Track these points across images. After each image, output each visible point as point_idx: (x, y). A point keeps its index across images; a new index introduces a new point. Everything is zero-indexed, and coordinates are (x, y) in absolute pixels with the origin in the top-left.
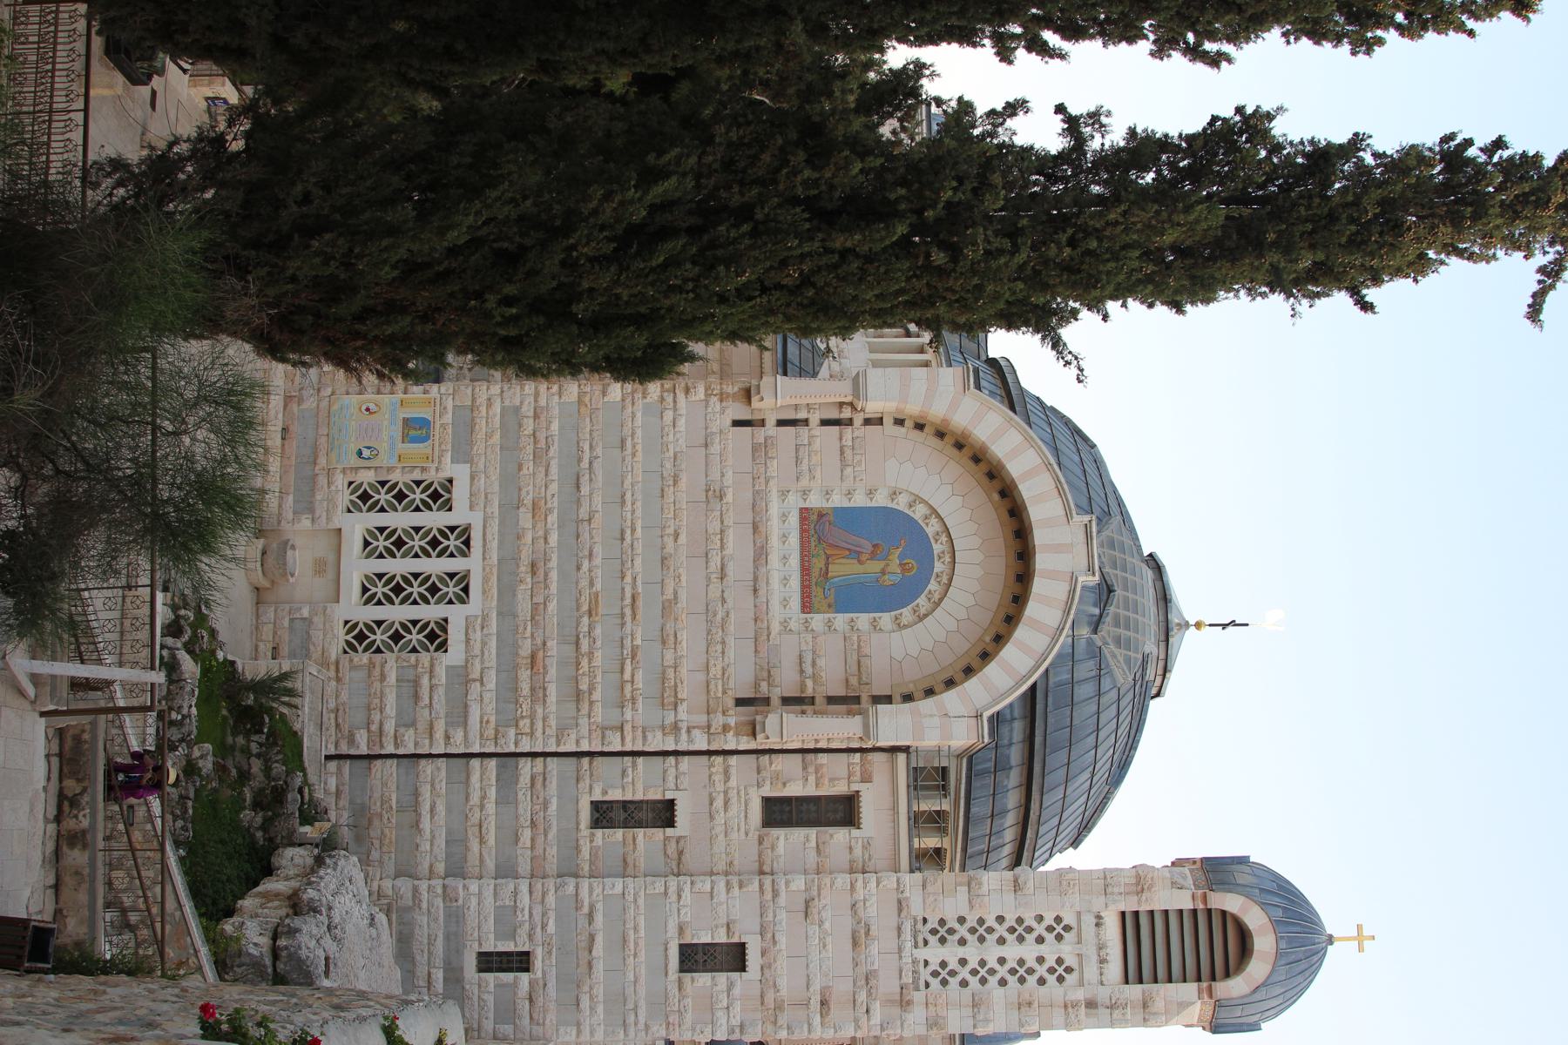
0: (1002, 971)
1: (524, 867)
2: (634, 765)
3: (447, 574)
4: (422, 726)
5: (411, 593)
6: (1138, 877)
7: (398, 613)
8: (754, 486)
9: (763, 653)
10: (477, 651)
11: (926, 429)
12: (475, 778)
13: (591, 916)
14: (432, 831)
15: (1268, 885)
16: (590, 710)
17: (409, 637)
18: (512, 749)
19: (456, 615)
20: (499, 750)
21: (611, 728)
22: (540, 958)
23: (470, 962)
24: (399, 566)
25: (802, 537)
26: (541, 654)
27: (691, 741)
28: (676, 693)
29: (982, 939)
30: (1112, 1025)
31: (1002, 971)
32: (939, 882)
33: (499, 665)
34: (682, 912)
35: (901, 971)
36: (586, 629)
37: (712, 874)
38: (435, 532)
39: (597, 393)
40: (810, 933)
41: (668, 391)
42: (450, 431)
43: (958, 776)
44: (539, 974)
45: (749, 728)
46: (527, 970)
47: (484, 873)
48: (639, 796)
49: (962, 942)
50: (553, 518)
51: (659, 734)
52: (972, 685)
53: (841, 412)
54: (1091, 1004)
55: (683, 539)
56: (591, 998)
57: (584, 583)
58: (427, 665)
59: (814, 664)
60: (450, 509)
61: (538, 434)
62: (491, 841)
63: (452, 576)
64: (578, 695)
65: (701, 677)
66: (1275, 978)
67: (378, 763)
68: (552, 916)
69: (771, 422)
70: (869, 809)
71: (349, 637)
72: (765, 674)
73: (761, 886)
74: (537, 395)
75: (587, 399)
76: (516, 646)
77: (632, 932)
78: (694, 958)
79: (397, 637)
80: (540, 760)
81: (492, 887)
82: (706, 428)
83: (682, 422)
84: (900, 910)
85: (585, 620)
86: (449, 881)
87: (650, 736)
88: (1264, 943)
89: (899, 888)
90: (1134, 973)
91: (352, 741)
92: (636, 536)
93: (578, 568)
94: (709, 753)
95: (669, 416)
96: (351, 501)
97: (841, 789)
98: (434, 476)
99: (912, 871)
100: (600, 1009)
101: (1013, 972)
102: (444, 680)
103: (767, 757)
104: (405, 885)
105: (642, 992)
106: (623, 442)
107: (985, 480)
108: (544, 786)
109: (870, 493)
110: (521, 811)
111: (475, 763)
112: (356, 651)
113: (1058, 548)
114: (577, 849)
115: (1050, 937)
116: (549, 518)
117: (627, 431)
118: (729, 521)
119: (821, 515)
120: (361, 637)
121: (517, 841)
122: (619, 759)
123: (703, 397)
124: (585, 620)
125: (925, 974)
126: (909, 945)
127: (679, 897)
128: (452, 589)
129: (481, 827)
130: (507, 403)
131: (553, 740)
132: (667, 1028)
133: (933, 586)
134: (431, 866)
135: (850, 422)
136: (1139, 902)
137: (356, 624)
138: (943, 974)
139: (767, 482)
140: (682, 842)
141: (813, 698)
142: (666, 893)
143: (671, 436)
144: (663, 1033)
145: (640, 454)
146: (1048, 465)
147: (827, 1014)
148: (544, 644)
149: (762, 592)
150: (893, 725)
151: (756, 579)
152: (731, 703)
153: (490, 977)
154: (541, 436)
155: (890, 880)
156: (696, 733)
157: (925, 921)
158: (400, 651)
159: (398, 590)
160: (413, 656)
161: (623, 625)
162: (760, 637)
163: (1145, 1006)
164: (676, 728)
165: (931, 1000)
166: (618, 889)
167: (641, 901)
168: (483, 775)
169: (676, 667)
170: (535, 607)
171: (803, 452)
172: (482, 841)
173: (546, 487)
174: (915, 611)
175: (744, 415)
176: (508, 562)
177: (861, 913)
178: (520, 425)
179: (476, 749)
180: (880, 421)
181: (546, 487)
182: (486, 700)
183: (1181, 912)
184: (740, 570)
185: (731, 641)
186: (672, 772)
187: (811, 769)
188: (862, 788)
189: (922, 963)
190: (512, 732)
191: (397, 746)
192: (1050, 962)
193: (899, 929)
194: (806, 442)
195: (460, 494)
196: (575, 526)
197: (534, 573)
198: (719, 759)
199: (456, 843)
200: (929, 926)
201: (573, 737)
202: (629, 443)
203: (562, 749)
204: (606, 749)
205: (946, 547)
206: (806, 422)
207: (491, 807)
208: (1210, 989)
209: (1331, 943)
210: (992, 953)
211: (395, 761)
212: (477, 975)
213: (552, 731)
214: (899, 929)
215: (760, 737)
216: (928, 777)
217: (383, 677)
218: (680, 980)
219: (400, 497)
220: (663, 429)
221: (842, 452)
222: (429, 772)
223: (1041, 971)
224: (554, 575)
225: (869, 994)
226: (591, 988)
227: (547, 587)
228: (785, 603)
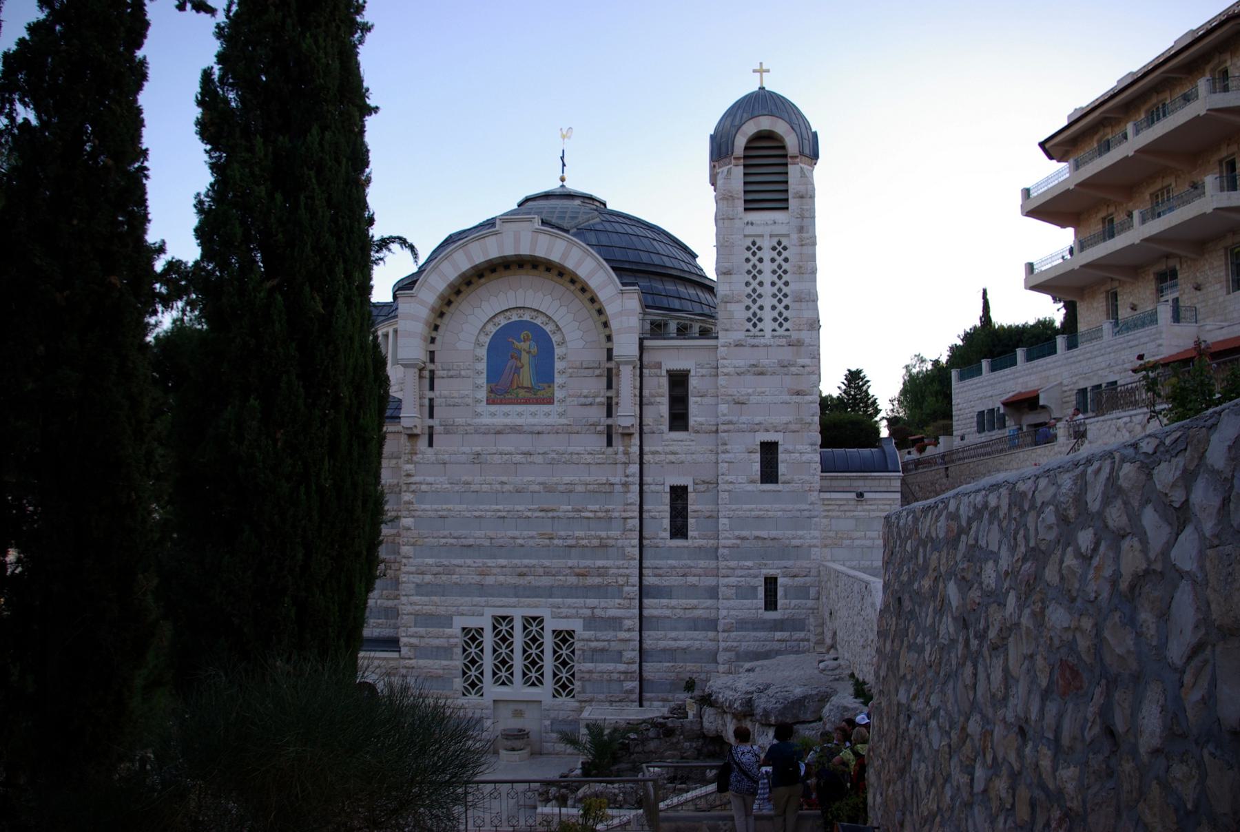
0: (780, 284)
1: (711, 581)
2: (649, 511)
3: (524, 631)
4: (619, 646)
5: (536, 654)
6: (722, 199)
7: (548, 663)
8: (471, 434)
9: (579, 428)
10: (574, 611)
11: (438, 323)
12: (655, 612)
13: (743, 538)
14: (688, 640)
15: (729, 119)
16: (613, 539)
17: (564, 656)
18: (637, 588)
19: (550, 625)
20: (638, 597)
21: (625, 524)
22: (768, 571)
23: (771, 615)
24: (518, 662)
25: (505, 404)
26: (577, 570)
27: (633, 475)
28: (602, 484)
29: (760, 296)
30: (813, 218)
31: (780, 284)
32: (725, 321)
33: (583, 597)
34: (741, 481)
35: (779, 346)
36: (561, 541)
37: (717, 463)
38: (496, 639)
39: (408, 534)
40: (755, 401)
41: (408, 488)
42: (430, 629)
43: (657, 315)
44: (779, 571)
45: (626, 438)
46: (776, 579)
47: (715, 606)
48: (668, 508)
49: (761, 308)
50: (490, 562)
51: (629, 495)
52: (602, 296)
53: (425, 378)
54: (801, 229)
55: (504, 479)
56: (794, 538)
57: (531, 542)
58: (582, 643)
59: (585, 397)
60: (482, 629)
61: (434, 572)
62: (695, 602)
63: (525, 628)
64: (603, 546)
65: (593, 468)
66: (787, 119)
67: (645, 674)
68: (741, 563)
69: (430, 422)
70: (678, 364)
71: (564, 694)
72: (592, 427)
73: (725, 431)
74: (408, 573)
75: (412, 540)
76: (571, 587)
77: (753, 513)
78: (769, 473)
79: (564, 664)
80: (645, 571)
81: (725, 601)
82: (433, 463)
83: (430, 479)
84: (742, 345)
85: (556, 542)
86: (720, 628)
87: (630, 501)
88: (765, 123)
89: (728, 345)
90: (781, 204)
91: (631, 691)
92: (502, 509)
93: (522, 546)
94: (641, 464)
95: (424, 487)
96: (476, 694)
97: (665, 382)
98: (459, 640)
99: (717, 338)
100: (800, 533)
101: (780, 277)
102: (592, 632)
103: (644, 428)
104: (721, 657)
105: (790, 507)
106: (441, 517)
107: (472, 287)
108: (661, 568)
109: (478, 359)
110: (676, 583)
111: (645, 613)
112: (573, 690)
113: (517, 240)
114: (700, 548)
115: (759, 254)
116: (489, 565)
117: (432, 514)
118: (493, 450)
119: (491, 391)
120: (564, 687)
121: (695, 586)
122: (645, 522)
123: (413, 466)
124: (556, 542)
125: (781, 331)
126: (763, 341)
127: (731, 483)
128: (534, 628)
129: (686, 609)
130: (413, 592)
131: (632, 562)
132: (813, 491)
133: (538, 322)
134: (710, 640)
135: (432, 372)
136: (739, 199)
137: (556, 690)
138: (780, 320)
139: (469, 425)
140: (697, 481)
141: (608, 398)
142: (729, 491)
143: (439, 486)
144: (816, 493)
145: (450, 506)
146: (465, 245)
147: (805, 391)
148: (570, 568)
149: (539, 429)
150: (626, 346)
151: (532, 433)
152: (610, 449)
153: (780, 602)
154: (436, 570)
155: (722, 351)
156: (628, 472)
157: (748, 330)
158: (573, 661)
159: (534, 663)
160: (576, 652)
161: (559, 518)
162: (568, 431)
163: (802, 197)
165: (797, 328)
166: (726, 521)
167: (734, 507)
168: (654, 607)
169: (587, 484)
170: (547, 574)
171: (451, 401)
172: (695, 608)
173: (469, 567)
174: (554, 333)
175: (424, 440)
176: (517, 591)
177: (742, 370)
178: (428, 584)
179: (637, 611)
180: (432, 353)
181: (469, 567)
182: (606, 605)
183: (745, 174)
184: (525, 443)
185: (570, 449)
186: (653, 488)
187: (652, 400)
188: (664, 368)
189: (774, 333)
190: (626, 589)
191: (634, 663)
192: (774, 254)
193: (753, 346)
194: (444, 400)
195: (473, 623)
196: (495, 549)
197: (525, 575)
198: (646, 458)
199: (695, 625)
200: (751, 328)
201: (630, 549)
202: (440, 513)
203: (637, 557)
204: (638, 529)
205: (514, 312)
206: (431, 400)
207: (674, 602)
208: (792, 157)
209: (764, 88)
210: (767, 290)
211: (644, 664)
212: (779, 611)
213: (626, 563)
214: (753, 346)
215: (632, 430)
216: (657, 329)
217: (590, 672)
218: (784, 483)
219: (473, 662)
220: (433, 491)
221: (451, 377)
222: (651, 642)
223: (779, 260)
224: (526, 562)
225: (793, 365)
226: (788, 538)
227: (534, 566)
228: (548, 414)
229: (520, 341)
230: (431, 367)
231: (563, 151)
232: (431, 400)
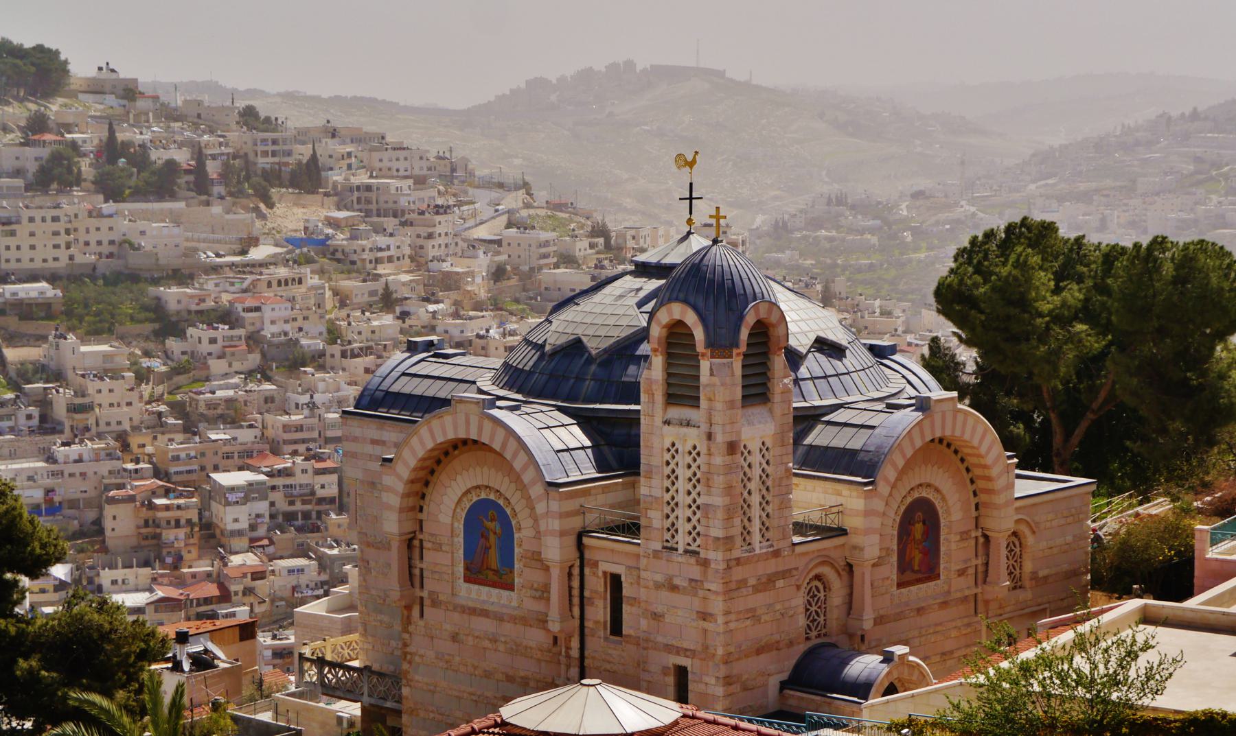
83: (422, 652)
119: (467, 568)
125: (693, 547)
135: (421, 541)
138: (694, 533)
206: (422, 570)
229: (487, 519)
230: (420, 537)
231: (691, 184)
232: (422, 570)
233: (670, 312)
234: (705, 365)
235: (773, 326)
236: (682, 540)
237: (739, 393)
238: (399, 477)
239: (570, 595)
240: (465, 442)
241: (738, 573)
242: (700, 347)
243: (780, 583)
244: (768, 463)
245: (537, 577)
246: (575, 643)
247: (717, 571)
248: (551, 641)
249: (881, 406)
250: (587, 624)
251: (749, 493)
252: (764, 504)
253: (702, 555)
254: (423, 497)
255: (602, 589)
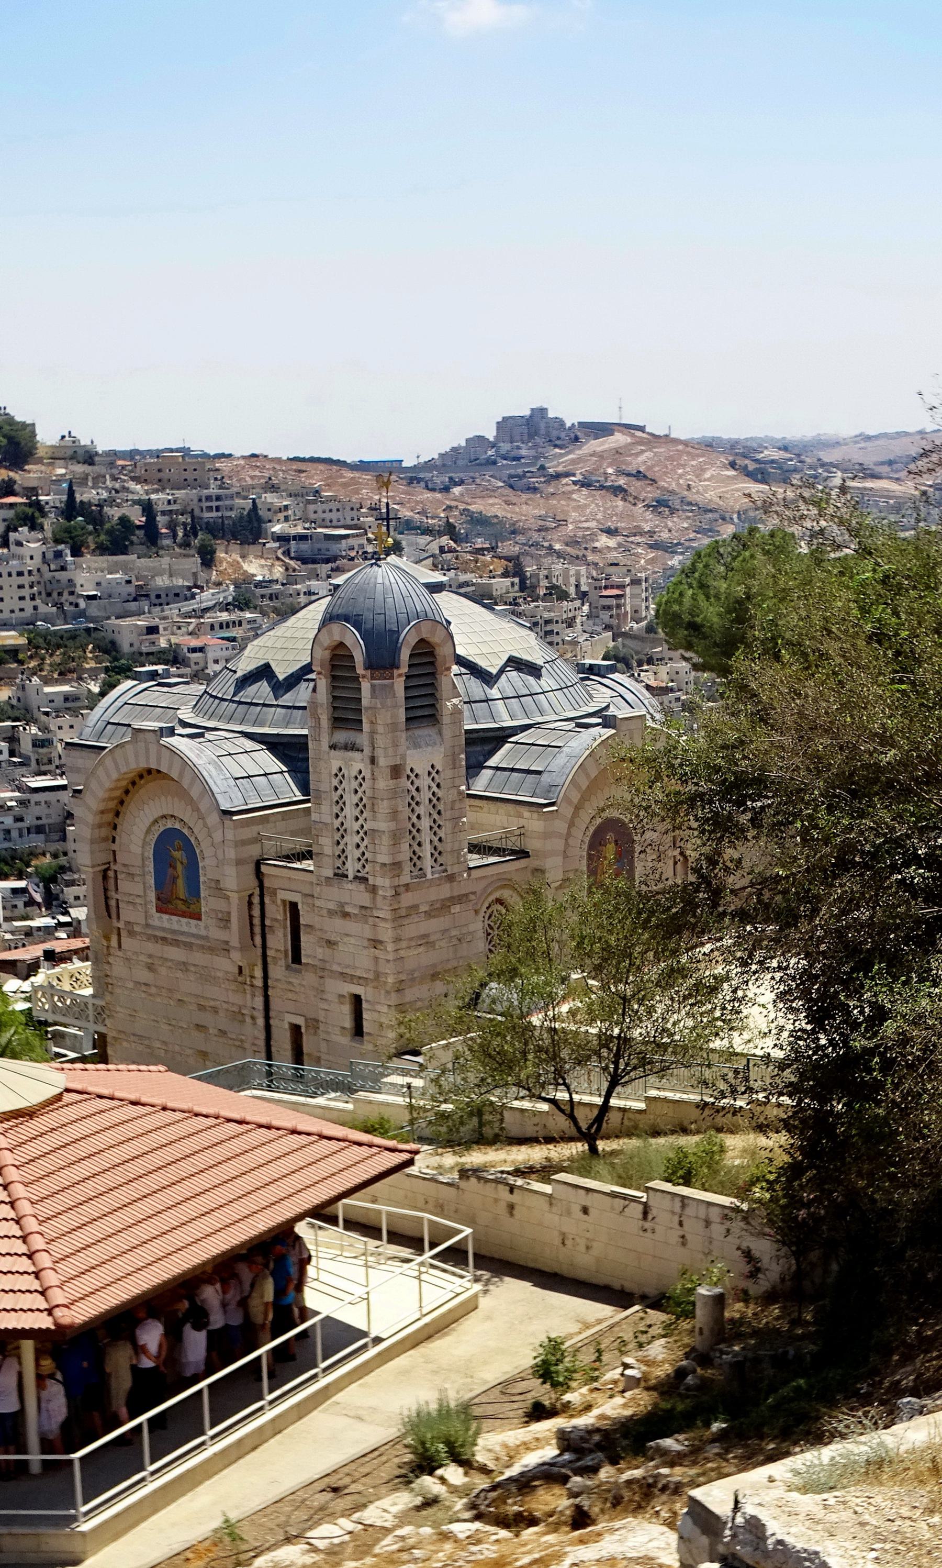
119: (158, 899)
152: (240, 979)
164: (253, 1018)
233: (330, 633)
234: (365, 686)
235: (439, 645)
236: (351, 868)
237: (402, 715)
238: (89, 808)
239: (251, 925)
240: (149, 771)
241: (407, 899)
242: (360, 670)
243: (456, 909)
244: (438, 786)
245: (221, 905)
246: (258, 973)
247: (385, 897)
248: (237, 971)
249: (571, 725)
250: (269, 953)
251: (419, 817)
252: (436, 828)
253: (371, 882)
254: (115, 827)
255: (280, 917)
